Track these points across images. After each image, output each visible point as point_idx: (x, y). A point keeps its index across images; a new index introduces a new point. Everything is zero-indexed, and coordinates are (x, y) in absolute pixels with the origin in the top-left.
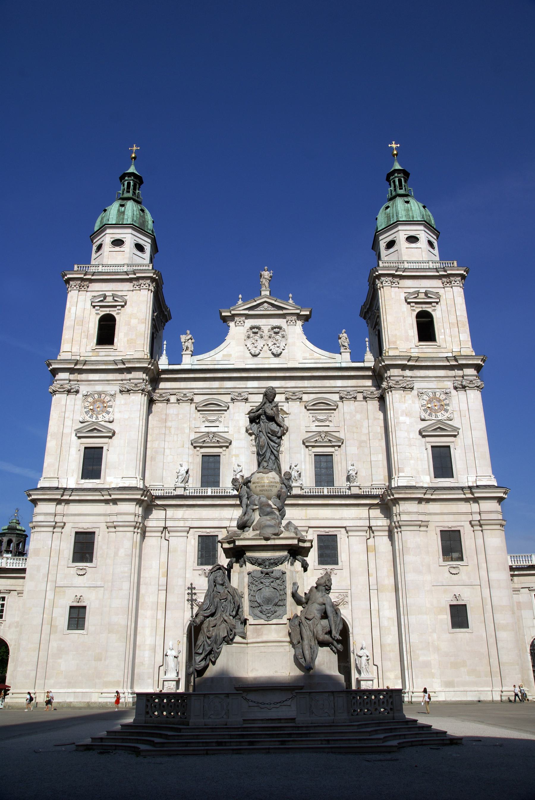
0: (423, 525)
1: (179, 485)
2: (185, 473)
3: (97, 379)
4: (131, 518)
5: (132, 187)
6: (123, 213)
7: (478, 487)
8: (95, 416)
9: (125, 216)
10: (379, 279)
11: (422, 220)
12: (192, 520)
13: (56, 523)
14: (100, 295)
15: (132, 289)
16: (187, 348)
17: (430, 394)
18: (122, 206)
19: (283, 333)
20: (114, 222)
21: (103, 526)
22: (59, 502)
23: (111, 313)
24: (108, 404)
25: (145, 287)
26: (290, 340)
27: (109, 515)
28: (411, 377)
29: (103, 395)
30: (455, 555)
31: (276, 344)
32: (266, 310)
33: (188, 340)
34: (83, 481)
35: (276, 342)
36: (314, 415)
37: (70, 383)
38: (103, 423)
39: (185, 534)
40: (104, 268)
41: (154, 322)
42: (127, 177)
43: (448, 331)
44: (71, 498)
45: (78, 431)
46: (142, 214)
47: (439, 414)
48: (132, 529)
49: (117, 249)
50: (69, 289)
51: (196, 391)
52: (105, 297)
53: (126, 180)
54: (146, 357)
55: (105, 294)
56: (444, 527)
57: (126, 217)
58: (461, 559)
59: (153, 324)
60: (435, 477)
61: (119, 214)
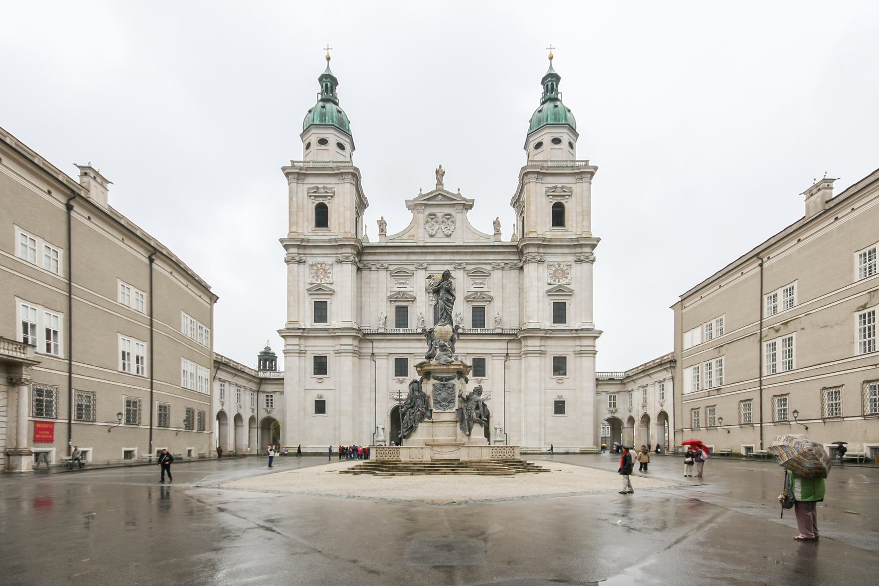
0: (542, 353)
1: (381, 326)
2: (385, 319)
4: (350, 348)
5: (329, 89)
7: (582, 329)
8: (319, 280)
10: (526, 176)
11: (566, 123)
12: (391, 348)
13: (300, 350)
17: (557, 266)
19: (452, 219)
21: (332, 352)
22: (300, 337)
24: (328, 271)
26: (458, 224)
27: (335, 345)
28: (544, 253)
30: (561, 372)
31: (446, 227)
32: (441, 200)
33: (383, 223)
34: (316, 324)
35: (447, 226)
36: (474, 280)
38: (325, 285)
39: (386, 357)
43: (575, 218)
44: (309, 335)
45: (309, 290)
47: (561, 280)
48: (351, 354)
49: (323, 147)
51: (390, 262)
53: (324, 82)
54: (353, 237)
56: (556, 355)
58: (565, 374)
60: (554, 323)
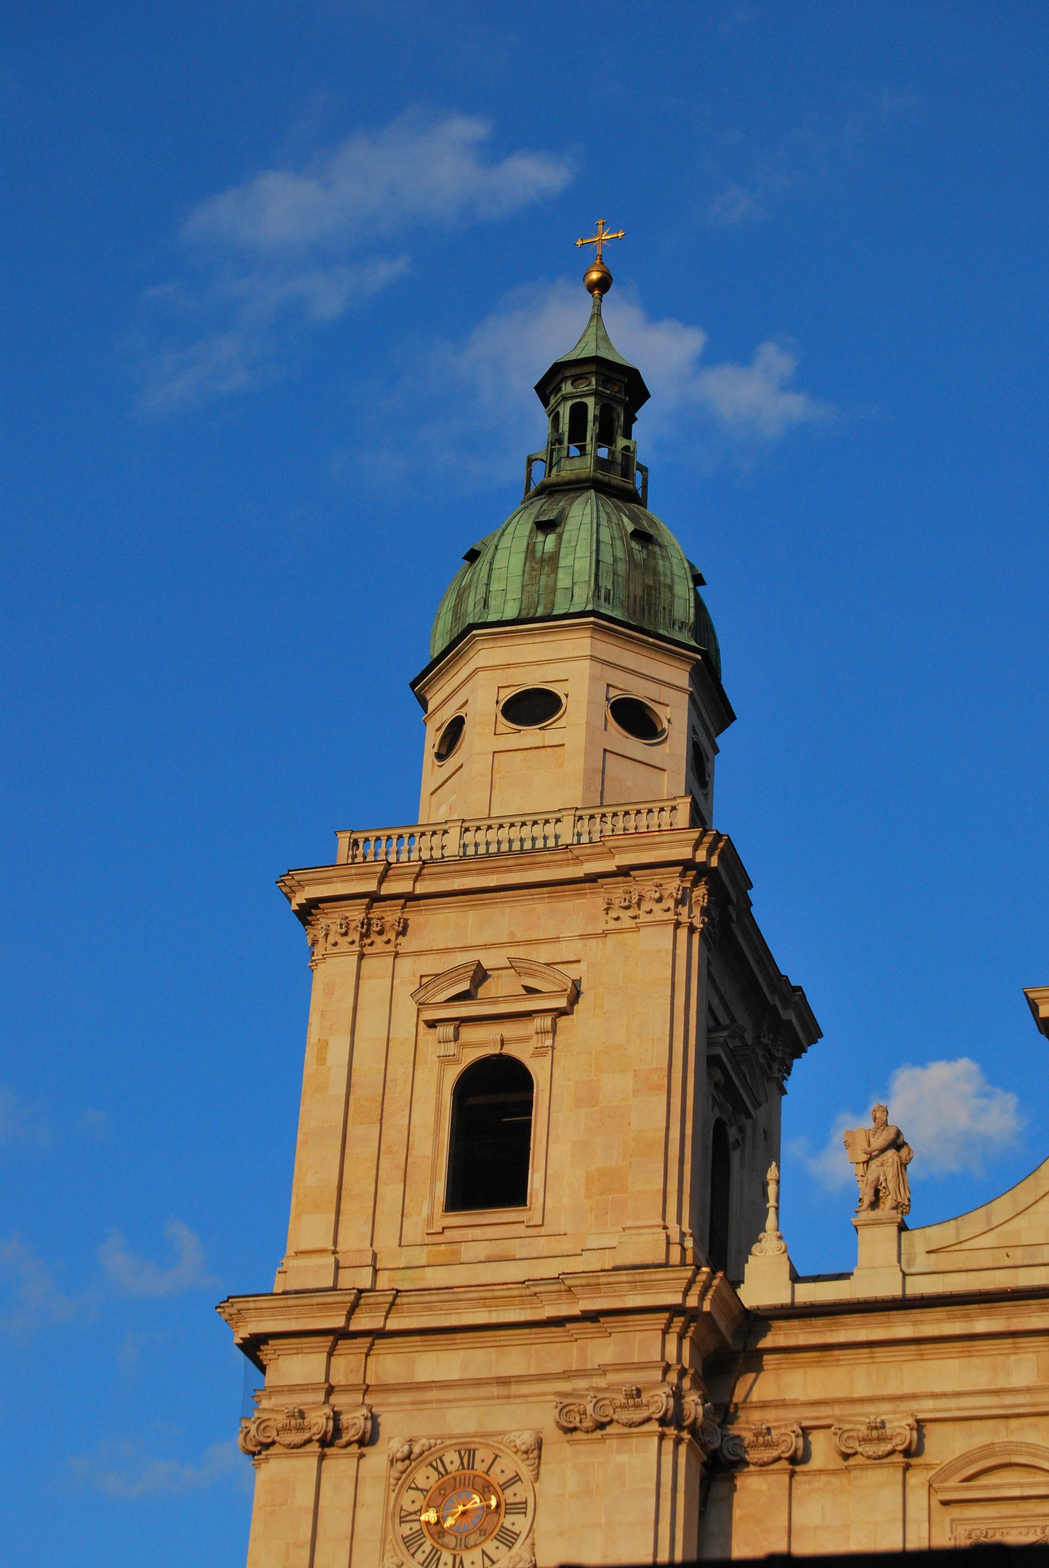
3: (455, 1376)
5: (591, 429)
6: (553, 560)
9: (560, 576)
14: (454, 970)
15: (601, 927)
16: (877, 1192)
18: (545, 527)
20: (511, 613)
23: (510, 1050)
24: (509, 1496)
25: (659, 915)
29: (479, 1456)
37: (333, 1399)
40: (469, 837)
41: (719, 1076)
42: (552, 397)
46: (640, 555)
49: (531, 735)
50: (319, 950)
52: (480, 975)
55: (479, 964)
57: (563, 581)
59: (717, 1086)
61: (533, 569)
